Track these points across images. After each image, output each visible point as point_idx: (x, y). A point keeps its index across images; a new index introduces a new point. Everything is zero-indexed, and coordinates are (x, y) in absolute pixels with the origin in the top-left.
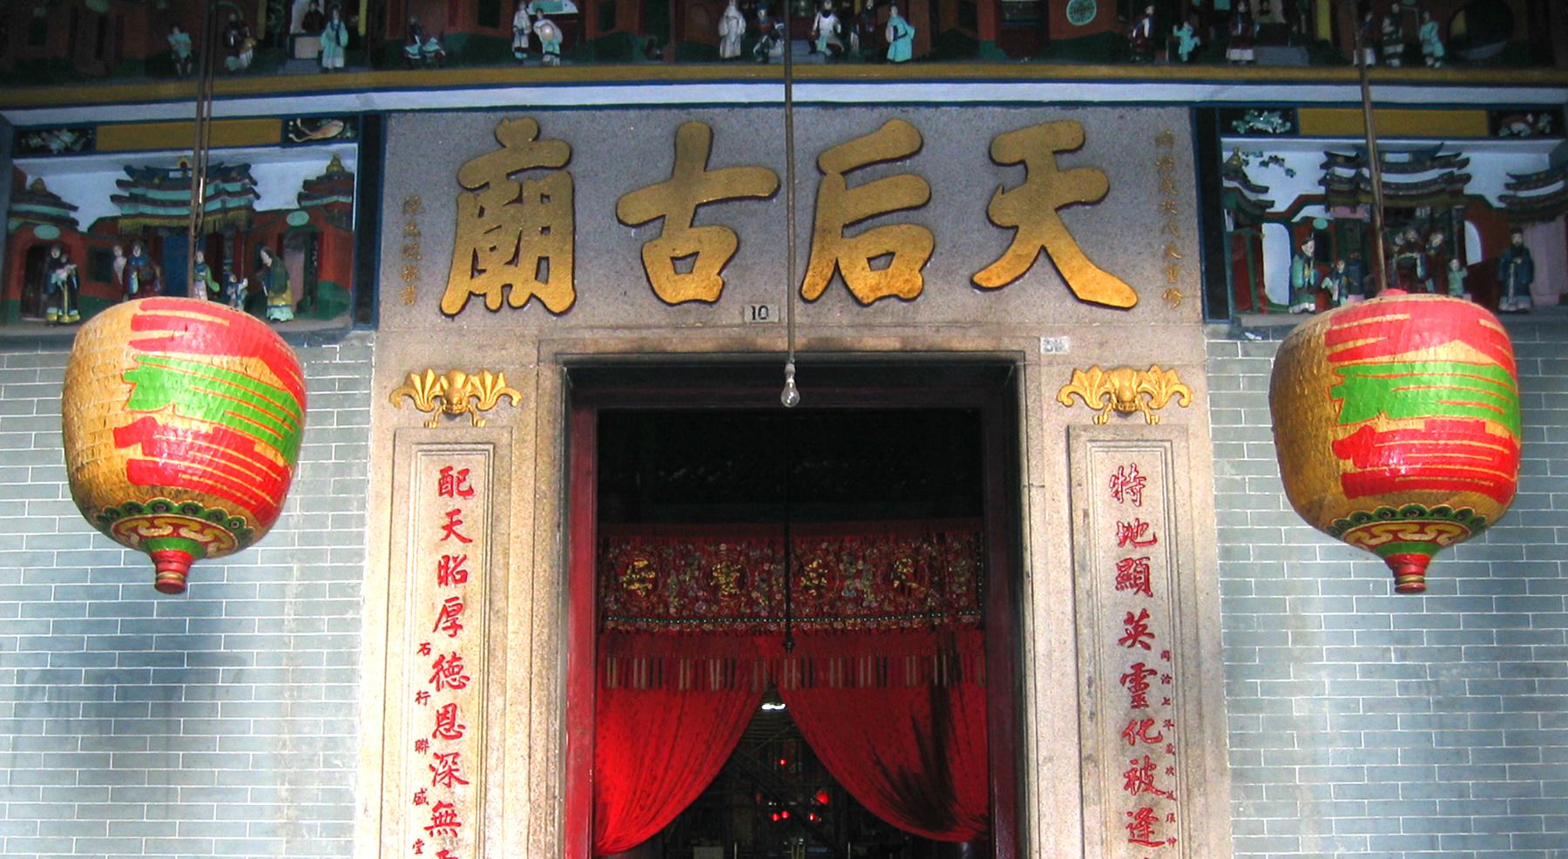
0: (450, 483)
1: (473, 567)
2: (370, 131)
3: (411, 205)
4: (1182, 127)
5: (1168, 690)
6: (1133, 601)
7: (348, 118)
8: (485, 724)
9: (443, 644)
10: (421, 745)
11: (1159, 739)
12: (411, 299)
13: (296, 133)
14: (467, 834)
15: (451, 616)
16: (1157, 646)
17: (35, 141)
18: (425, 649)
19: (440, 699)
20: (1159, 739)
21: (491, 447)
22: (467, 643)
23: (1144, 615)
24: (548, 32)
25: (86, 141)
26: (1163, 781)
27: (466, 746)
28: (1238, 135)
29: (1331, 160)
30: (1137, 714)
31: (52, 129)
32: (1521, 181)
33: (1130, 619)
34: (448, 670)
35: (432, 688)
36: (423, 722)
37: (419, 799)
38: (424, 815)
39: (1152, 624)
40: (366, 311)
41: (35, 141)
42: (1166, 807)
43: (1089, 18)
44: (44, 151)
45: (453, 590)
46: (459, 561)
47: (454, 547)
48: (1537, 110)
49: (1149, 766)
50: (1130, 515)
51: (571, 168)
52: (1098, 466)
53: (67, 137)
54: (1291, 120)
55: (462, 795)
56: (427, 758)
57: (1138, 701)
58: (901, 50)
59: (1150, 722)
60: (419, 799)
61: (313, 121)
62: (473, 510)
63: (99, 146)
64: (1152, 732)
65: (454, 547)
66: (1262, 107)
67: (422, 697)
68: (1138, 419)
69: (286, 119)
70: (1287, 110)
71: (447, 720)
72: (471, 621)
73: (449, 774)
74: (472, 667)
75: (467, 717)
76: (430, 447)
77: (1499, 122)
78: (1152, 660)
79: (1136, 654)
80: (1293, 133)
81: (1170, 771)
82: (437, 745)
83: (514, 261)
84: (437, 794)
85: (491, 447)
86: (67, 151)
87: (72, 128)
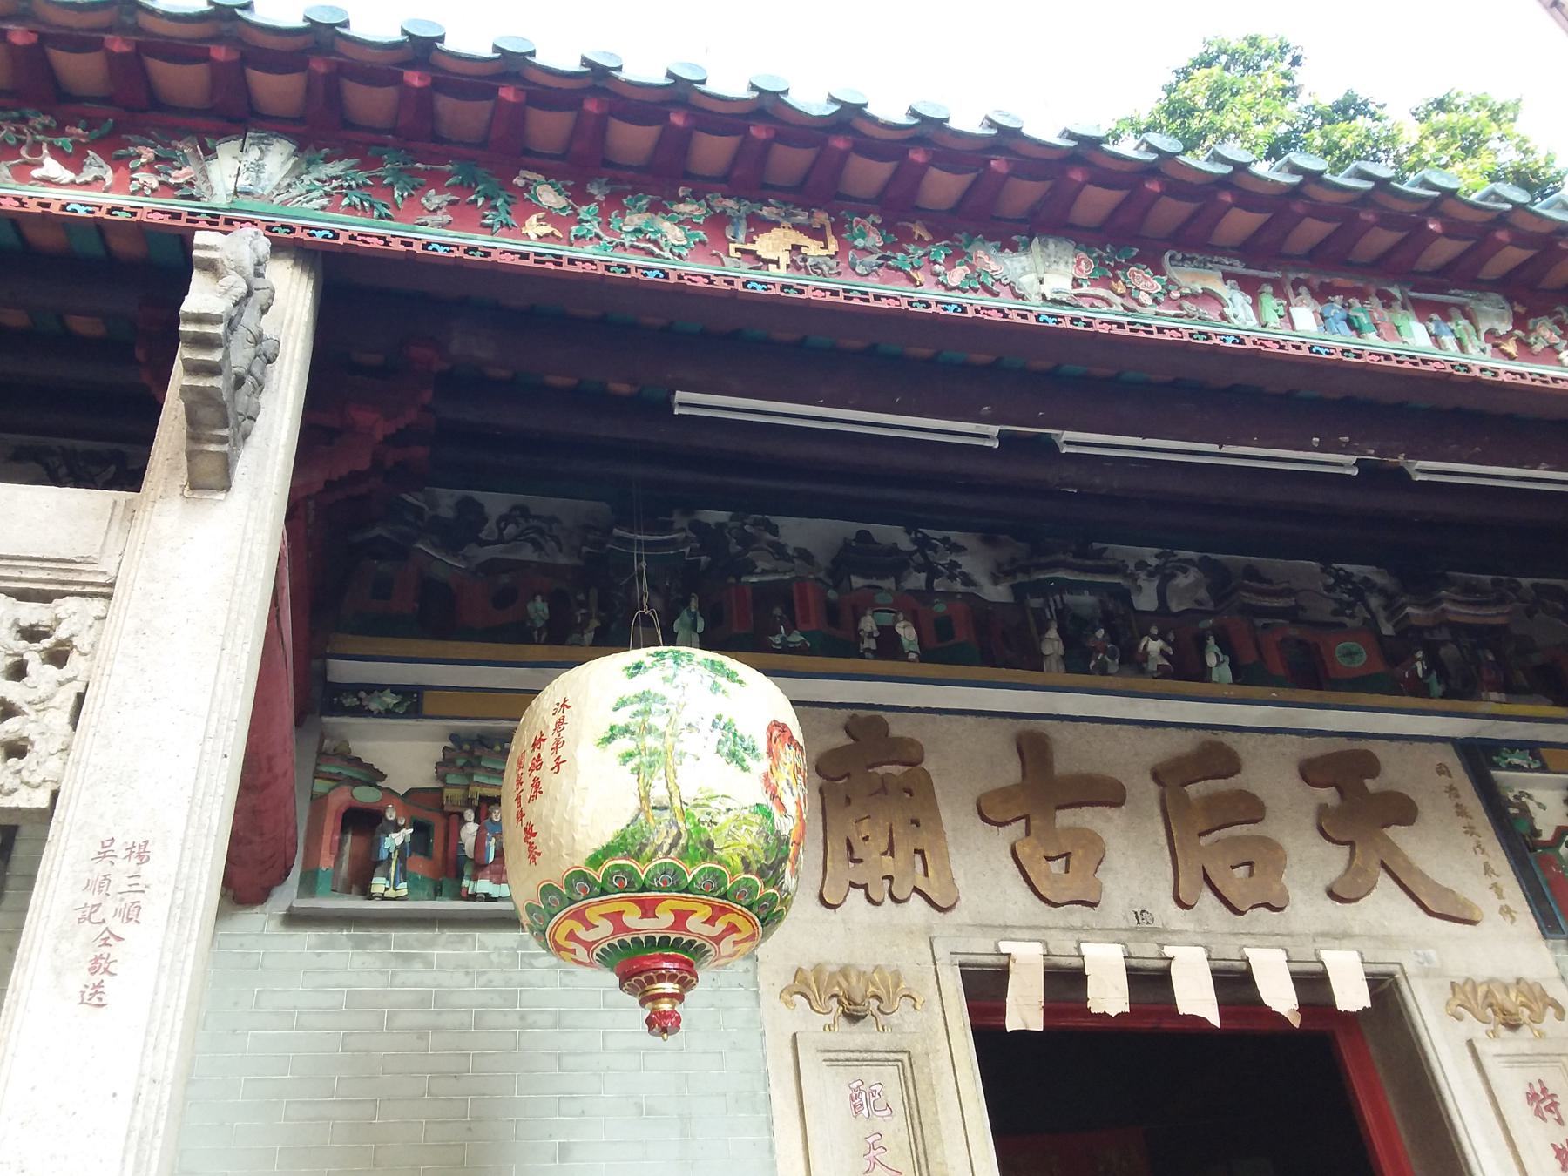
0: (858, 1101)
17: (350, 701)
21: (904, 1057)
28: (1497, 767)
31: (374, 689)
41: (350, 701)
43: (1344, 662)
44: (361, 711)
51: (923, 765)
52: (1512, 1086)
53: (390, 699)
63: (427, 709)
66: (1514, 745)
68: (1525, 1031)
70: (1532, 747)
80: (1544, 768)
83: (891, 850)
85: (904, 1057)
86: (389, 713)
87: (396, 689)
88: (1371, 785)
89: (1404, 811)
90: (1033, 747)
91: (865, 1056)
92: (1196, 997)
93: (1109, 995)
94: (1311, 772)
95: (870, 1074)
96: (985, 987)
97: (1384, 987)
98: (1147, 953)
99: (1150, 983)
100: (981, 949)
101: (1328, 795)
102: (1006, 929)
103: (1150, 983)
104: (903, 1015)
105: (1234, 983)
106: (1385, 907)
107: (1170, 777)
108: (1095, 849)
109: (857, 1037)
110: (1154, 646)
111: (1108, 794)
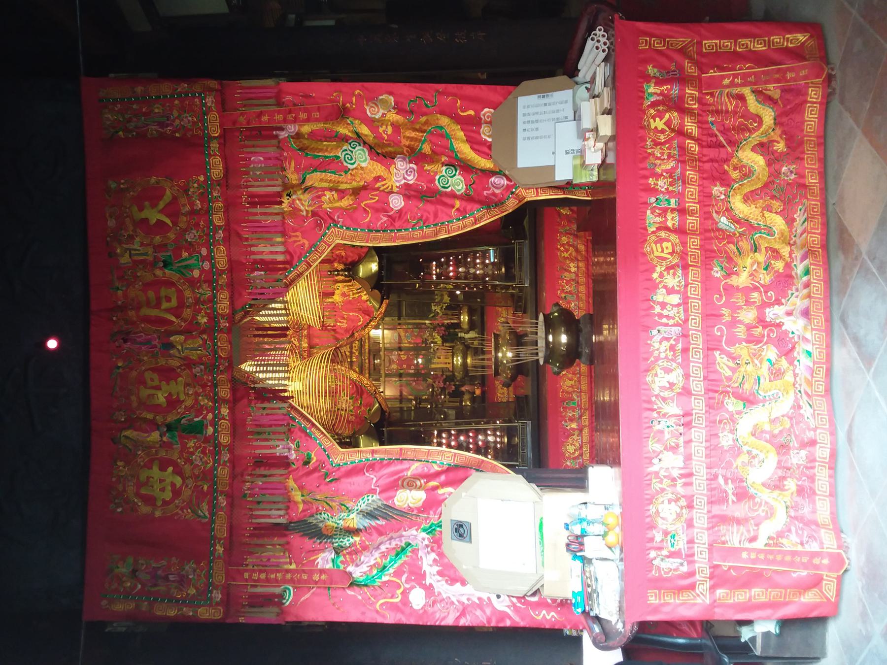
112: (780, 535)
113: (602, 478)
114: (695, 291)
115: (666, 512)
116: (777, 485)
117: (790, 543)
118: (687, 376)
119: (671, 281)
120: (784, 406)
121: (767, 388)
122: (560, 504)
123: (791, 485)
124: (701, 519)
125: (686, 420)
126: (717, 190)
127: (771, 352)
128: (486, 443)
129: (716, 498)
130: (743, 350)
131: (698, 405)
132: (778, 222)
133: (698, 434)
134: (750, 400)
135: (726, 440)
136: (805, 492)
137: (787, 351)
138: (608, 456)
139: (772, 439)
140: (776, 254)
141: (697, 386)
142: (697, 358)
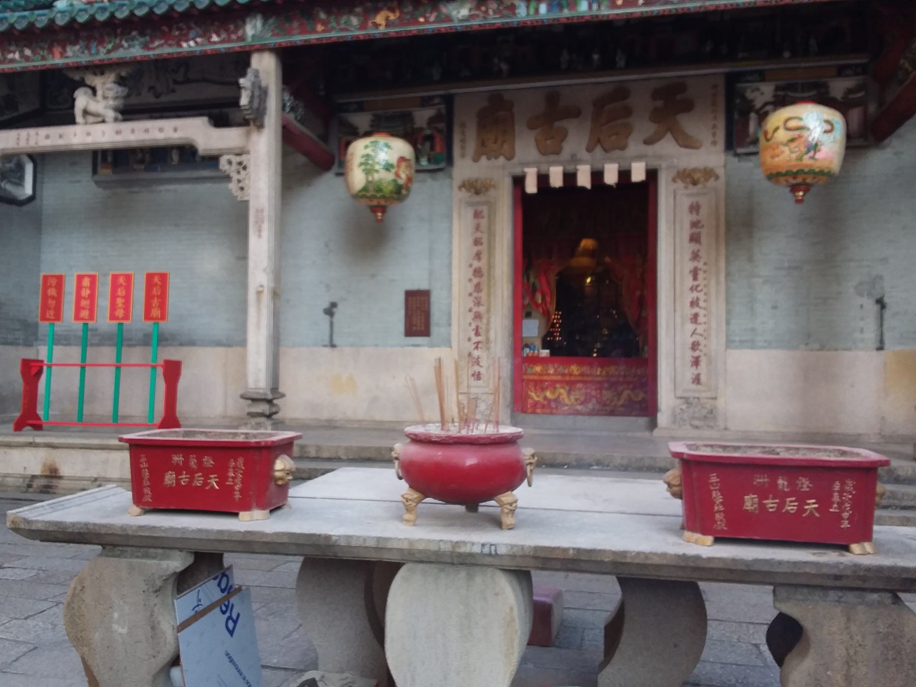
0: (477, 215)
1: (485, 240)
2: (449, 100)
3: (463, 125)
4: (721, 82)
5: (705, 275)
6: (694, 247)
7: (441, 96)
8: (489, 287)
9: (476, 264)
10: (470, 295)
11: (702, 290)
12: (463, 156)
13: (425, 102)
14: (485, 321)
15: (478, 256)
16: (702, 261)
18: (471, 266)
19: (475, 281)
20: (702, 290)
22: (483, 264)
23: (699, 250)
24: (504, 67)
25: (361, 108)
26: (702, 304)
27: (483, 295)
29: (777, 89)
30: (696, 283)
32: (850, 91)
33: (693, 252)
34: (477, 272)
35: (473, 278)
36: (470, 288)
37: (470, 310)
38: (471, 315)
39: (701, 254)
40: (450, 161)
42: (702, 312)
44: (347, 111)
45: (479, 248)
46: (481, 238)
47: (479, 235)
48: (857, 65)
49: (698, 299)
50: (694, 218)
54: (762, 77)
55: (482, 309)
56: (472, 299)
57: (695, 278)
58: (621, 63)
59: (698, 286)
60: (470, 310)
61: (431, 98)
62: (484, 222)
64: (699, 288)
65: (479, 235)
66: (752, 72)
67: (470, 280)
68: (700, 186)
69: (422, 98)
71: (478, 288)
72: (484, 257)
73: (478, 303)
74: (485, 270)
75: (484, 287)
76: (470, 204)
77: (841, 72)
78: (700, 265)
79: (695, 264)
81: (705, 301)
82: (475, 294)
84: (475, 309)
86: (355, 111)
87: (357, 103)
88: (679, 97)
89: (688, 107)
90: (552, 98)
91: (478, 203)
92: (584, 180)
93: (556, 181)
94: (656, 94)
95: (480, 208)
96: (519, 182)
97: (652, 174)
98: (570, 168)
99: (570, 177)
100: (517, 171)
101: (660, 103)
102: (528, 164)
103: (570, 177)
104: (492, 192)
105: (597, 176)
106: (667, 147)
107: (599, 104)
108: (564, 135)
109: (477, 199)
110: (596, 57)
111: (574, 113)
112: (532, 399)
113: (545, 353)
114: (600, 379)
115: (538, 369)
116: (545, 398)
117: (530, 401)
118: (576, 376)
119: (604, 373)
120: (567, 401)
121: (572, 397)
122: (538, 343)
123: (546, 403)
124: (536, 377)
125: (563, 375)
126: (631, 386)
127: (582, 399)
128: (556, 337)
129: (542, 381)
130: (583, 391)
131: (567, 378)
132: (621, 402)
133: (559, 378)
134: (569, 393)
135: (558, 385)
136: (543, 407)
137: (582, 403)
138: (552, 354)
139: (558, 397)
140: (612, 401)
141: (573, 378)
142: (580, 378)
